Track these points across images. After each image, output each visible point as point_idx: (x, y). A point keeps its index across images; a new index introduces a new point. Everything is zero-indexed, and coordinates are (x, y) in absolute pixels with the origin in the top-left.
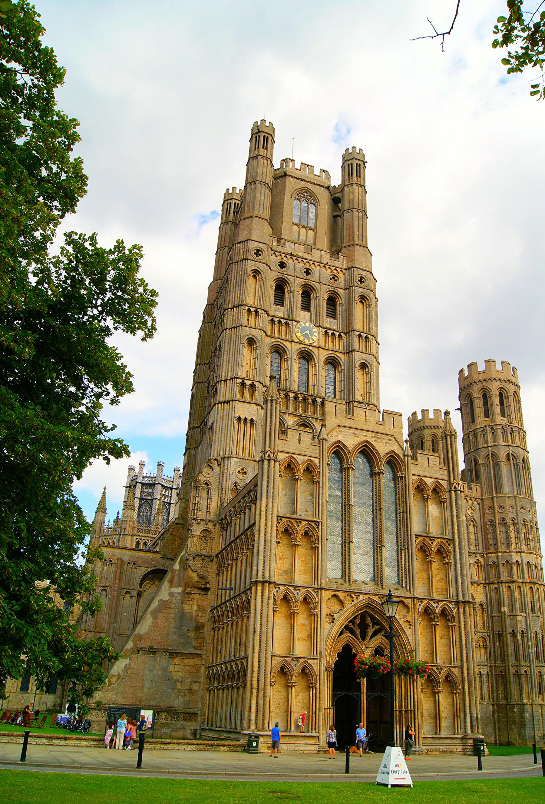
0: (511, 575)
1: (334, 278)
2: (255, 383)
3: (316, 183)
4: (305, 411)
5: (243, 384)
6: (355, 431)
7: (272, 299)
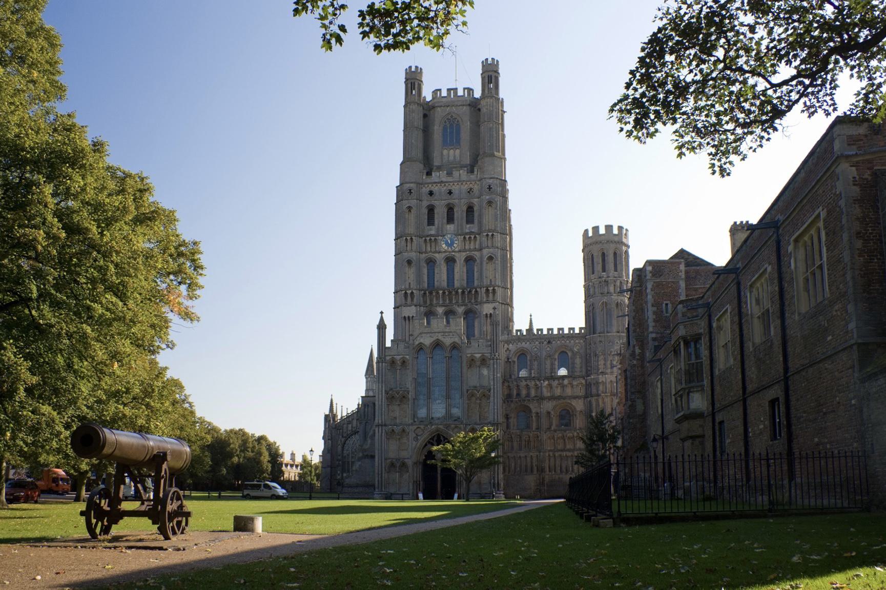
0: (598, 391)
1: (470, 191)
2: (414, 291)
3: (460, 103)
4: (451, 300)
5: (406, 293)
6: (431, 335)
7: (426, 221)
